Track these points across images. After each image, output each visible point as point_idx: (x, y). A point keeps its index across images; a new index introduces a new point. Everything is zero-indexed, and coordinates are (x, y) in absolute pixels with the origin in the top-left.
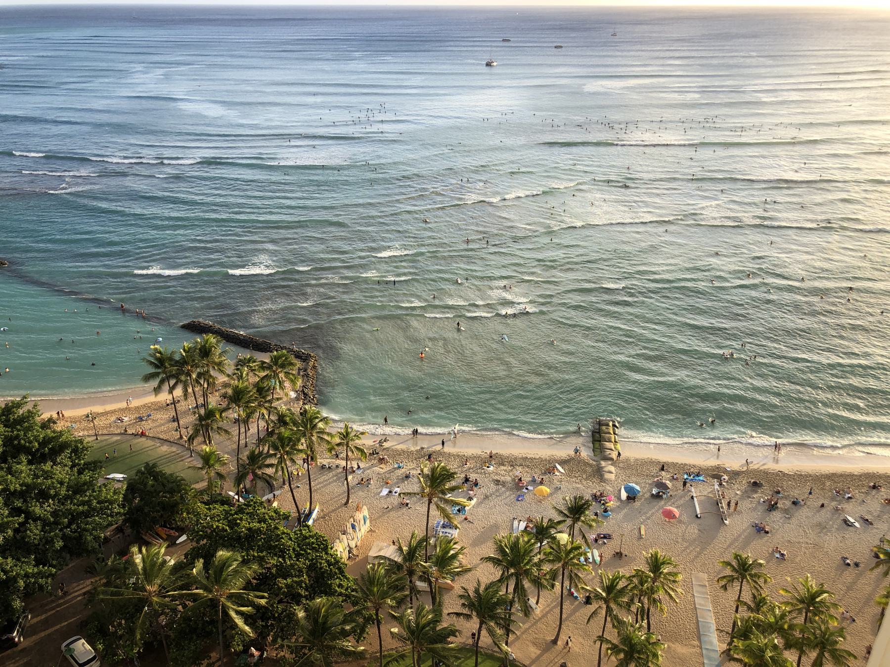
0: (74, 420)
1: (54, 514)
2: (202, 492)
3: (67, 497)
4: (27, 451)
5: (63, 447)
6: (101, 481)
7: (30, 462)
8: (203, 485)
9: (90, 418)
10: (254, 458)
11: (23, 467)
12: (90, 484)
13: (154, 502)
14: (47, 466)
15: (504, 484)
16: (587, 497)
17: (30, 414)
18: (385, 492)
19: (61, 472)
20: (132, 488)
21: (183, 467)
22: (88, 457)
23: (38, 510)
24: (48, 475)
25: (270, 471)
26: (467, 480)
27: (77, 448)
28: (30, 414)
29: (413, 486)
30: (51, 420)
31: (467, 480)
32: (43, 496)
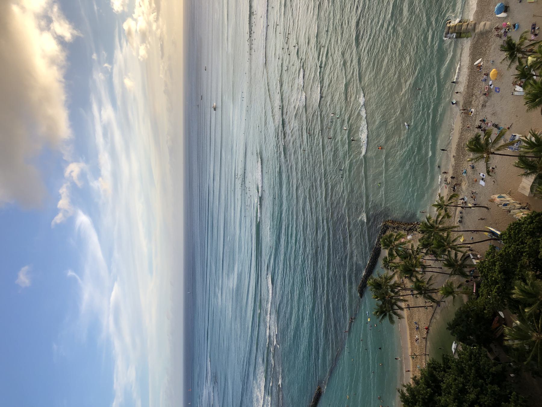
0: (415, 366)
1: (475, 386)
2: (470, 299)
3: (465, 378)
4: (432, 395)
5: (431, 375)
6: (456, 357)
7: (440, 395)
8: (465, 298)
9: (414, 356)
10: (450, 264)
11: (443, 400)
12: (458, 363)
13: (474, 326)
14: (444, 386)
15: (485, 102)
16: (500, 42)
17: (409, 389)
18: (482, 183)
19: (448, 379)
20: (462, 339)
21: (450, 307)
22: (441, 361)
23: (473, 396)
24: (449, 386)
25: (460, 255)
26: (480, 127)
27: (433, 367)
28: (409, 389)
29: (481, 165)
30: (414, 378)
31: (480, 127)
32: (463, 391)
